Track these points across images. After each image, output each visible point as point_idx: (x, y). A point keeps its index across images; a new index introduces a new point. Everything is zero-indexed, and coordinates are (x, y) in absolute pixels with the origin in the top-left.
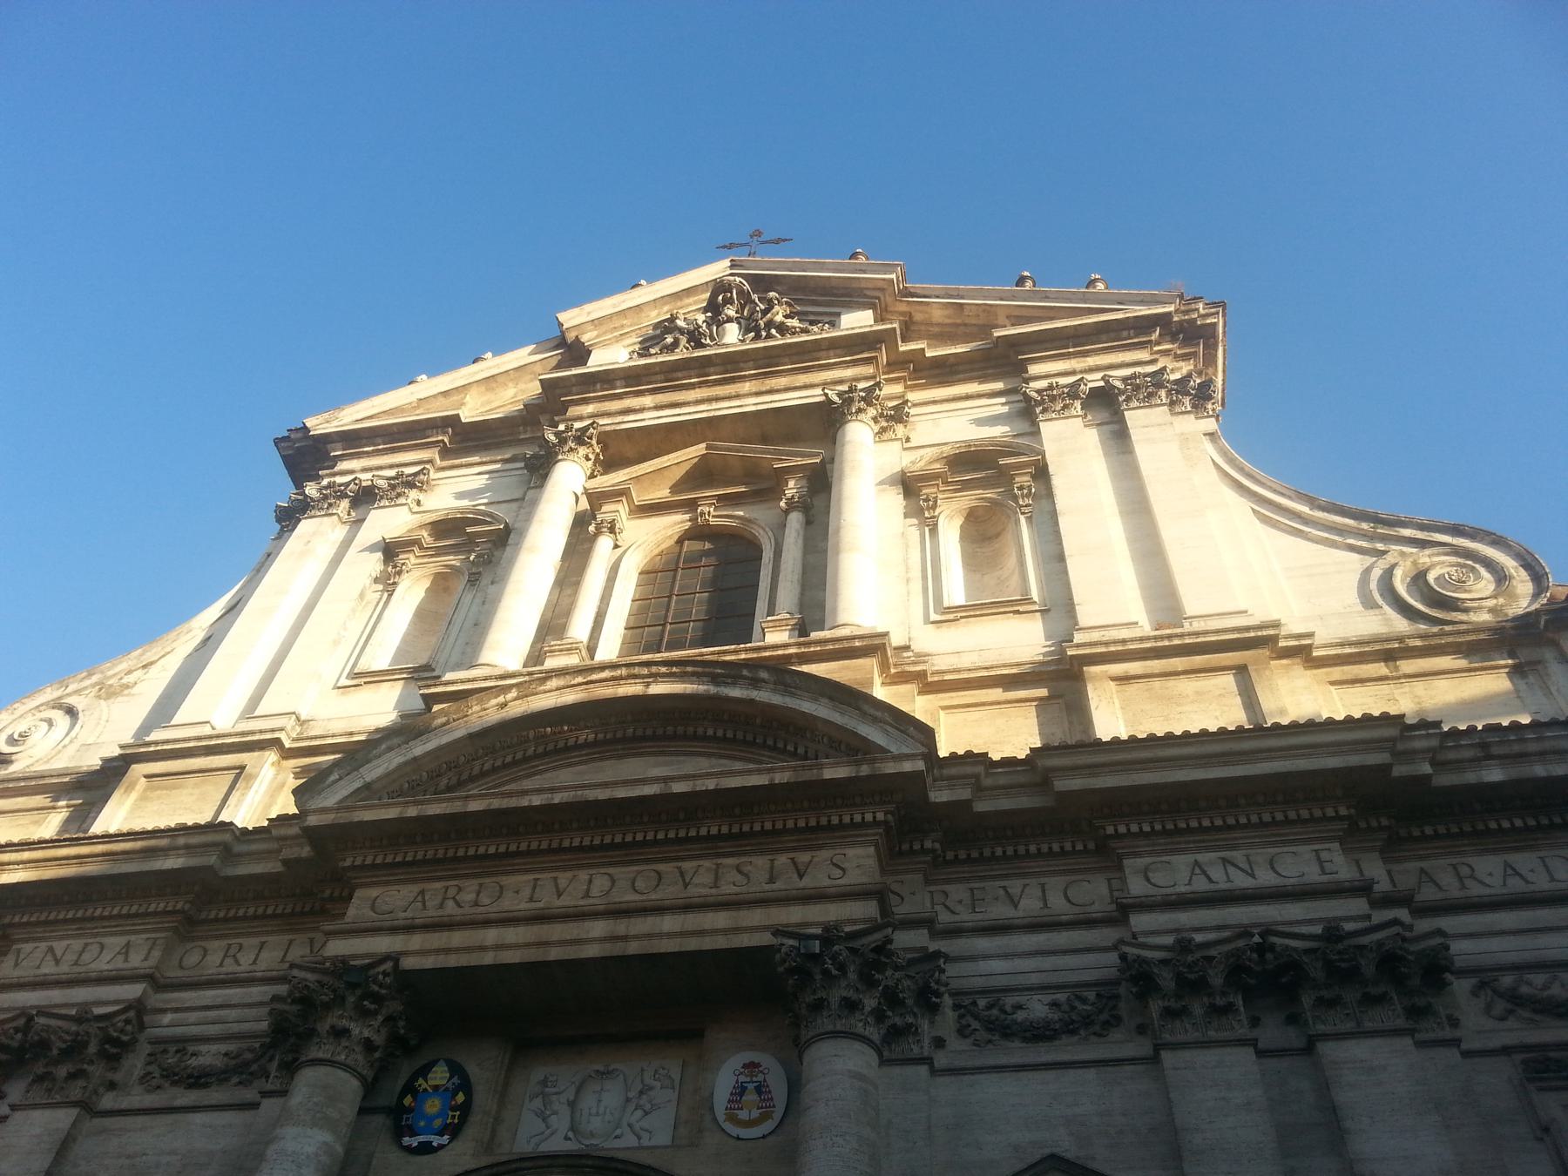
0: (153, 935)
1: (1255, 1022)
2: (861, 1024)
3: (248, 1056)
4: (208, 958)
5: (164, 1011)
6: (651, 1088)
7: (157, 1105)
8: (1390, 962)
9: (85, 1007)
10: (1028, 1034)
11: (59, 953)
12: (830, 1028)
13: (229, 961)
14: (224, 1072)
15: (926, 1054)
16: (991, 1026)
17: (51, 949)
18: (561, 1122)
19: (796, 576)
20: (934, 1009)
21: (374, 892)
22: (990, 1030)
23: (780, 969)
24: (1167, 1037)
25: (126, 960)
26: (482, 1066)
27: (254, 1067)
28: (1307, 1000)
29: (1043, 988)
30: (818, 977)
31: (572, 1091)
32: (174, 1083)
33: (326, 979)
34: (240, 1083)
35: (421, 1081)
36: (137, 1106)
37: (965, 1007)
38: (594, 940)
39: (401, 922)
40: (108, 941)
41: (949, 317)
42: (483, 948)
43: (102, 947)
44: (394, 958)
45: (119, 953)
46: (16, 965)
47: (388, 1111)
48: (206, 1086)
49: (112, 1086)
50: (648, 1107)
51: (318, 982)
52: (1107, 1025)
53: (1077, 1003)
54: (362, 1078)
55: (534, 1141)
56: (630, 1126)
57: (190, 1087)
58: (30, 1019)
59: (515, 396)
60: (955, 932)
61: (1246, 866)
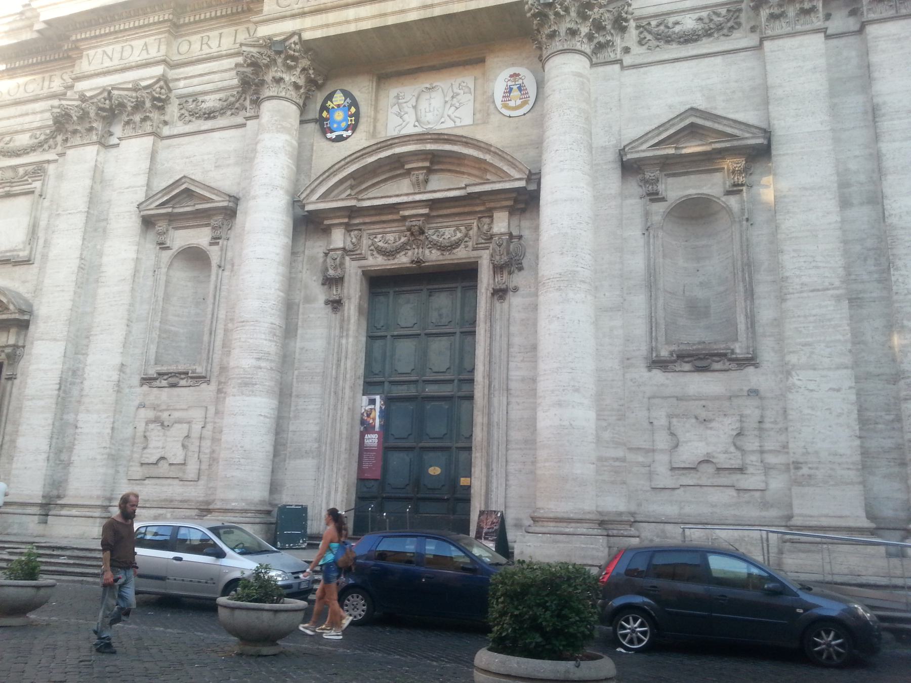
0: (160, 36)
1: (828, 17)
2: (579, 44)
3: (233, 99)
4: (192, 47)
6: (458, 94)
7: (192, 131)
9: (136, 83)
10: (682, 40)
11: (110, 54)
12: (561, 48)
13: (205, 47)
14: (222, 109)
15: (618, 57)
16: (658, 37)
17: (104, 52)
18: (410, 118)
20: (623, 30)
22: (658, 39)
23: (529, 15)
24: (769, 32)
25: (148, 53)
26: (362, 90)
27: (237, 105)
29: (693, 10)
30: (552, 17)
31: (414, 99)
32: (197, 118)
33: (262, 50)
34: (232, 114)
35: (329, 103)
36: (182, 132)
37: (643, 27)
38: (413, 9)
39: (296, 11)
40: (133, 43)
42: (348, 22)
43: (132, 48)
44: (298, 34)
45: (142, 50)
46: (90, 64)
47: (315, 121)
48: (214, 117)
49: (166, 123)
50: (457, 105)
51: (259, 53)
52: (732, 28)
53: (716, 19)
54: (297, 104)
55: (399, 128)
56: (449, 116)
57: (206, 119)
58: (109, 93)
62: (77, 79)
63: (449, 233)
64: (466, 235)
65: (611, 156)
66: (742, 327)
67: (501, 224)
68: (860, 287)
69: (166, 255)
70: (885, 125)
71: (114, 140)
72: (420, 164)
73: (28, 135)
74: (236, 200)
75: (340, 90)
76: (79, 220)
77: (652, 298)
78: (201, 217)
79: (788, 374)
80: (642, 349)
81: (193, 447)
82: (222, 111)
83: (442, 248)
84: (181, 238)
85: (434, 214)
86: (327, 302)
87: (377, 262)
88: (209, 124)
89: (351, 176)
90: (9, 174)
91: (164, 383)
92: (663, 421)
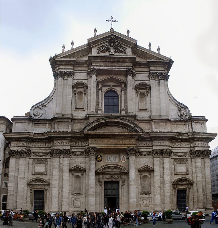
8: (169, 152)
18: (109, 160)
19: (124, 102)
21: (91, 140)
28: (164, 154)
41: (141, 53)
42: (103, 147)
59: (81, 55)
62: (54, 146)
63: (116, 177)
65: (137, 169)
69: (73, 176)
75: (100, 155)
76: (58, 170)
78: (80, 171)
82: (80, 155)
84: (76, 174)
87: (106, 180)
90: (40, 160)
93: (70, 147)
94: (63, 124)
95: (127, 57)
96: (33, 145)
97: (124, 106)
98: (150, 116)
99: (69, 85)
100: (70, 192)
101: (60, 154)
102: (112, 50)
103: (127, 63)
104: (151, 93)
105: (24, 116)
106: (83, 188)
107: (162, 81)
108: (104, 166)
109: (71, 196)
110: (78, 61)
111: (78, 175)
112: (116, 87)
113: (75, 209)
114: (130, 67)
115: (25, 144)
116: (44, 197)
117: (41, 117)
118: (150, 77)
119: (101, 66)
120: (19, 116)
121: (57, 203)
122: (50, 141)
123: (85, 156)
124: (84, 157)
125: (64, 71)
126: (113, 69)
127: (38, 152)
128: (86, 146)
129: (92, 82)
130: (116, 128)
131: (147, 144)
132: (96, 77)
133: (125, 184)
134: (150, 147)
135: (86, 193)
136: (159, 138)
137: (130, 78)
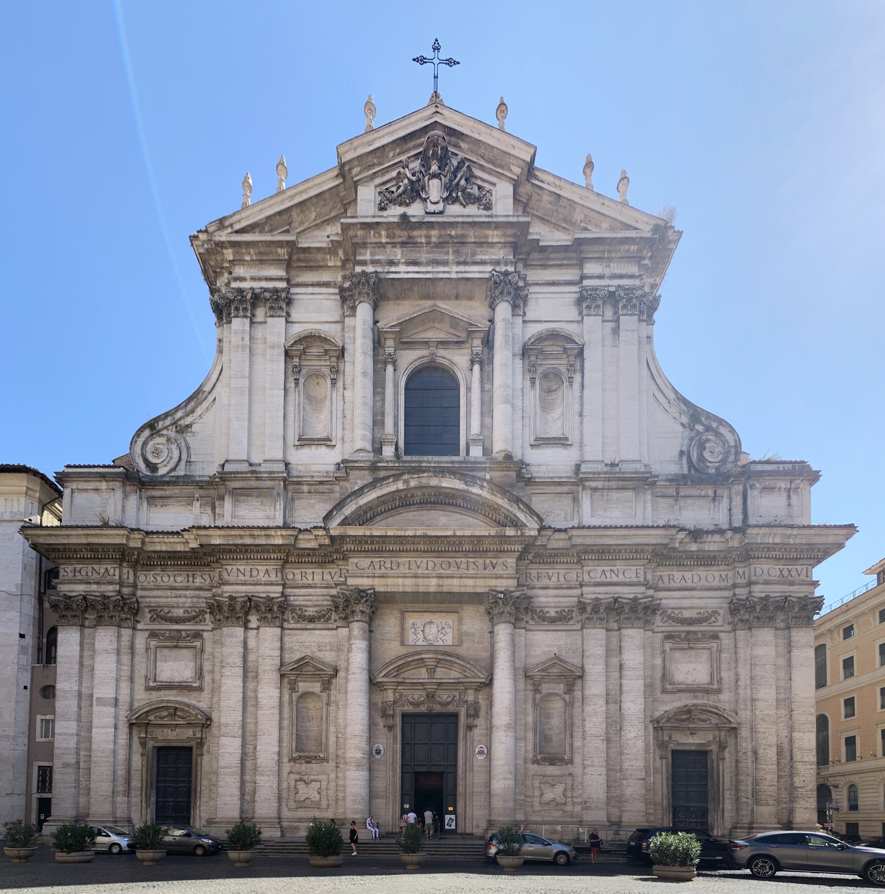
3: (323, 612)
5: (290, 596)
17: (238, 569)
20: (527, 613)
40: (258, 567)
46: (229, 575)
48: (314, 621)
49: (285, 620)
60: (533, 588)
61: (616, 573)
64: (453, 699)
65: (521, 672)
66: (567, 749)
67: (470, 697)
68: (609, 736)
70: (624, 673)
71: (251, 625)
72: (433, 664)
73: (182, 611)
74: (336, 671)
76: (239, 671)
77: (535, 734)
79: (584, 768)
80: (530, 755)
81: (324, 793)
82: (319, 618)
83: (442, 704)
84: (303, 686)
85: (440, 688)
86: (384, 726)
87: (409, 709)
88: (311, 626)
89: (399, 666)
91: (303, 761)
92: (537, 785)
93: (280, 589)
94: (255, 502)
95: (495, 220)
96: (146, 578)
97: (482, 426)
98: (578, 467)
99: (273, 347)
100: (285, 751)
101: (247, 614)
102: (435, 189)
103: (492, 247)
104: (585, 372)
105: (109, 466)
106: (327, 737)
107: (628, 322)
108: (399, 658)
109: (287, 767)
110: (303, 244)
111: (310, 690)
112: (449, 351)
113: (301, 814)
114: (506, 264)
115: (112, 570)
116: (194, 769)
117: (173, 474)
118: (584, 305)
119: (391, 263)
120: (85, 467)
121: (237, 792)
122: (208, 565)
123: (335, 621)
124: (330, 626)
125: (252, 289)
126: (441, 276)
127: (166, 607)
128: (339, 585)
129: (359, 333)
130: (445, 515)
131: (562, 579)
132: (375, 307)
133: (480, 722)
134: (570, 588)
135: (337, 756)
136: (603, 553)
137: (503, 309)
